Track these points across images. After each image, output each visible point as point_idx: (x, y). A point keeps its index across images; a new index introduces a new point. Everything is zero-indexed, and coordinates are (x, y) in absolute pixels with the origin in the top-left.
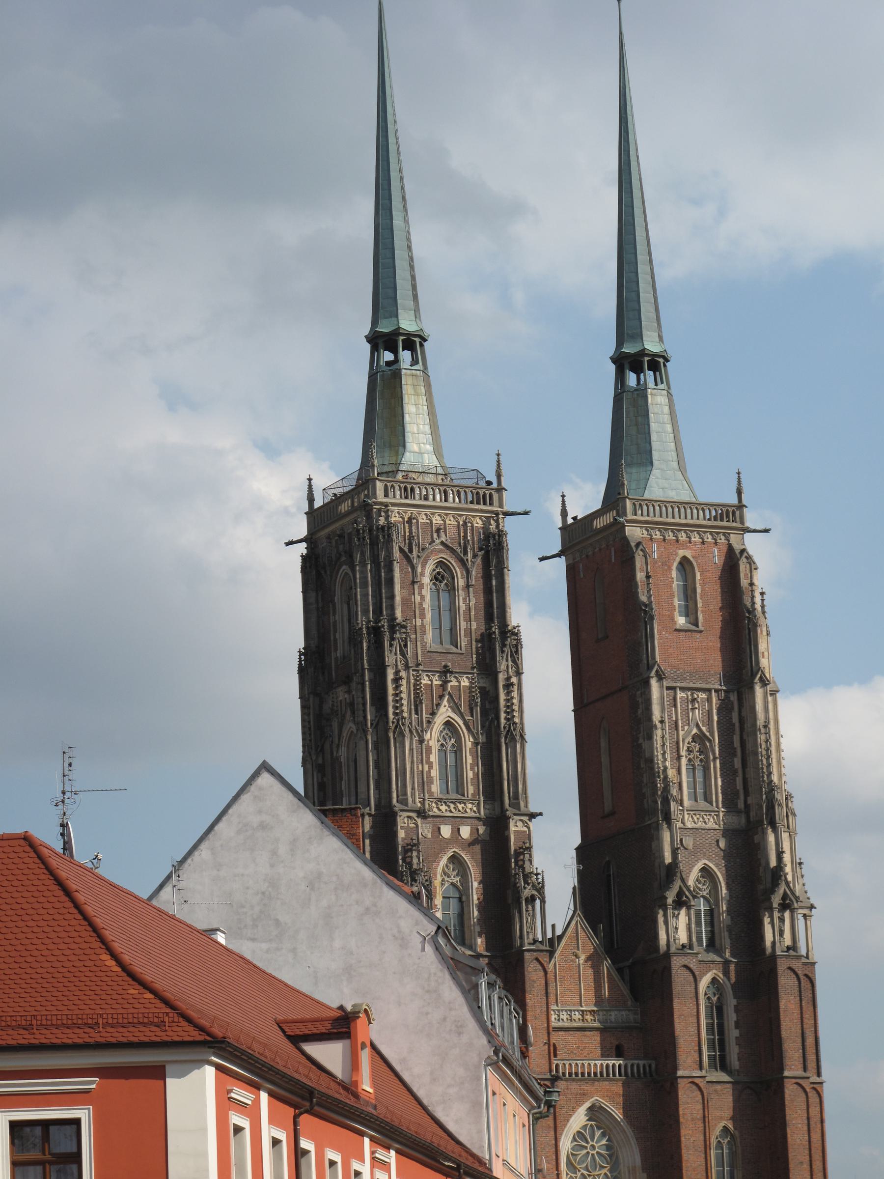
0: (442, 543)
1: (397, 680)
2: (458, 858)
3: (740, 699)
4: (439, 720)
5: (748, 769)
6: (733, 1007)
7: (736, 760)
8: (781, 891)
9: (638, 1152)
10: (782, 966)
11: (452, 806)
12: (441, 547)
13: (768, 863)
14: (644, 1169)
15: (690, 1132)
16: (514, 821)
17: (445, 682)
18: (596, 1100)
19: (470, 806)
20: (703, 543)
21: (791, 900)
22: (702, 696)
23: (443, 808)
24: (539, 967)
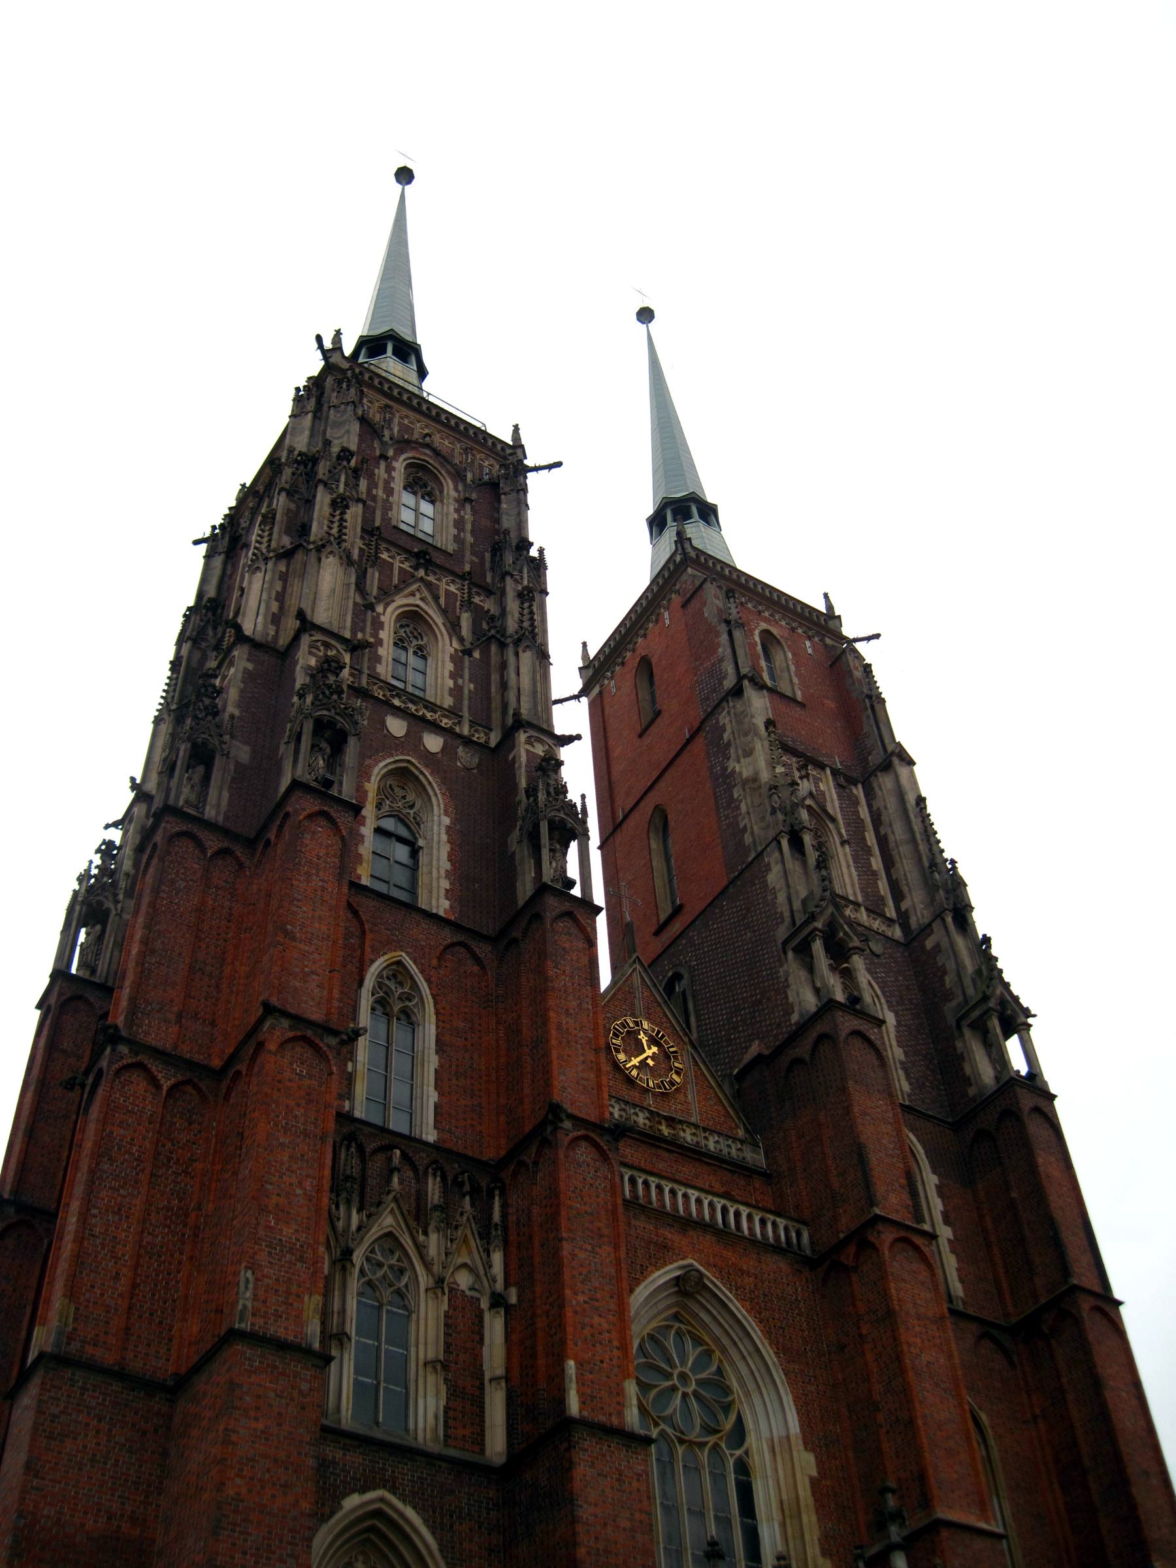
0: (428, 446)
1: (340, 504)
2: (417, 778)
3: (870, 794)
4: (401, 601)
5: (898, 865)
6: (933, 1187)
7: (873, 860)
8: (998, 992)
9: (792, 1403)
10: (1027, 1101)
11: (410, 705)
12: (428, 452)
13: (960, 967)
14: (808, 1444)
15: (918, 1340)
16: (528, 735)
17: (416, 568)
18: (691, 1265)
19: (445, 721)
20: (793, 630)
21: (1013, 1010)
22: (812, 771)
23: (396, 702)
24: (574, 930)
